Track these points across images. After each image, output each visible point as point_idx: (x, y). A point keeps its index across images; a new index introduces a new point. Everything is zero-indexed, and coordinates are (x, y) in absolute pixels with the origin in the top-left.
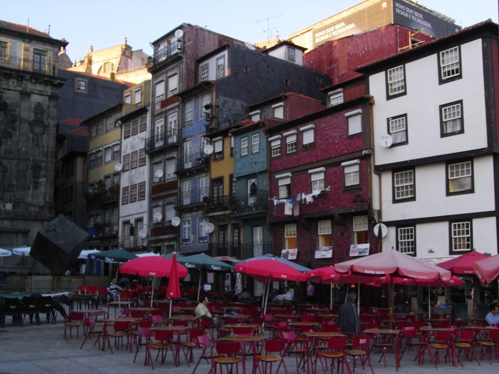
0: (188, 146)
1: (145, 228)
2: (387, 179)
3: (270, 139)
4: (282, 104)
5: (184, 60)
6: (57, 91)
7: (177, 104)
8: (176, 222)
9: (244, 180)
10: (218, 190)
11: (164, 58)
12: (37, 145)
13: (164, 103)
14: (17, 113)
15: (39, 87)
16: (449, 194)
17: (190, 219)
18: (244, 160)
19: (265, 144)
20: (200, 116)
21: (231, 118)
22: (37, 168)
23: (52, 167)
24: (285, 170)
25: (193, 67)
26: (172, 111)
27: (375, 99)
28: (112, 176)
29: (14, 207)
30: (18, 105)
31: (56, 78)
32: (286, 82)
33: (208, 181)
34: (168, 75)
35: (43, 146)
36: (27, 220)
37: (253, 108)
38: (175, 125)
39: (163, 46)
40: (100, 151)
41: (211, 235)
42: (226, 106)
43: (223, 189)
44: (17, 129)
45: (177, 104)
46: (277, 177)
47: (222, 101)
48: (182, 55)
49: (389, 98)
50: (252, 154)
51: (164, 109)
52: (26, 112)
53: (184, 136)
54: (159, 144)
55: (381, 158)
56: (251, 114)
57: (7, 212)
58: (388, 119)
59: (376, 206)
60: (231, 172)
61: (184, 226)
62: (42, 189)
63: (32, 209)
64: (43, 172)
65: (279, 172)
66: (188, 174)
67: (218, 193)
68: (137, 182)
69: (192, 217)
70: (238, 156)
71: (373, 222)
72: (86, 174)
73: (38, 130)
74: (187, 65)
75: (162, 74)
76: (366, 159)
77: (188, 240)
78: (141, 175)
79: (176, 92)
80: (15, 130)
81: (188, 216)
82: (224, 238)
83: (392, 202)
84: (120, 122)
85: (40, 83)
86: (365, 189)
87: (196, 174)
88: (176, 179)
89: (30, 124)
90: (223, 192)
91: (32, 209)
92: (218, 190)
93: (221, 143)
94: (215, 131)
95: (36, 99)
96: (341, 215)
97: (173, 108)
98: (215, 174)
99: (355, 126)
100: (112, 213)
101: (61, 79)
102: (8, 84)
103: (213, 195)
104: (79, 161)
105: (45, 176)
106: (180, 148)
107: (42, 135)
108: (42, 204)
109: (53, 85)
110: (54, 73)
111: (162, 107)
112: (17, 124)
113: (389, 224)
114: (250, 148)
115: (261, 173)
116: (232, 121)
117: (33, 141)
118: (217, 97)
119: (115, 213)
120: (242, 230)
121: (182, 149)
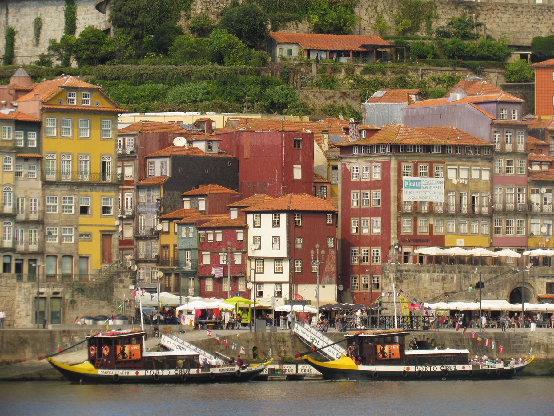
0: (142, 218)
5: (137, 158)
7: (133, 187)
8: (135, 268)
10: (166, 252)
16: (275, 273)
17: (144, 267)
19: (196, 234)
24: (206, 251)
25: (143, 162)
26: (129, 191)
33: (158, 245)
38: (131, 202)
41: (161, 279)
53: (139, 211)
55: (250, 254)
60: (175, 243)
61: (140, 271)
67: (166, 254)
69: (146, 266)
70: (180, 236)
74: (140, 161)
76: (244, 253)
77: (143, 280)
79: (132, 179)
82: (169, 281)
88: (132, 239)
90: (169, 254)
92: (166, 252)
97: (129, 189)
98: (163, 243)
99: (240, 237)
103: (162, 254)
114: (187, 233)
115: (193, 249)
118: (164, 193)
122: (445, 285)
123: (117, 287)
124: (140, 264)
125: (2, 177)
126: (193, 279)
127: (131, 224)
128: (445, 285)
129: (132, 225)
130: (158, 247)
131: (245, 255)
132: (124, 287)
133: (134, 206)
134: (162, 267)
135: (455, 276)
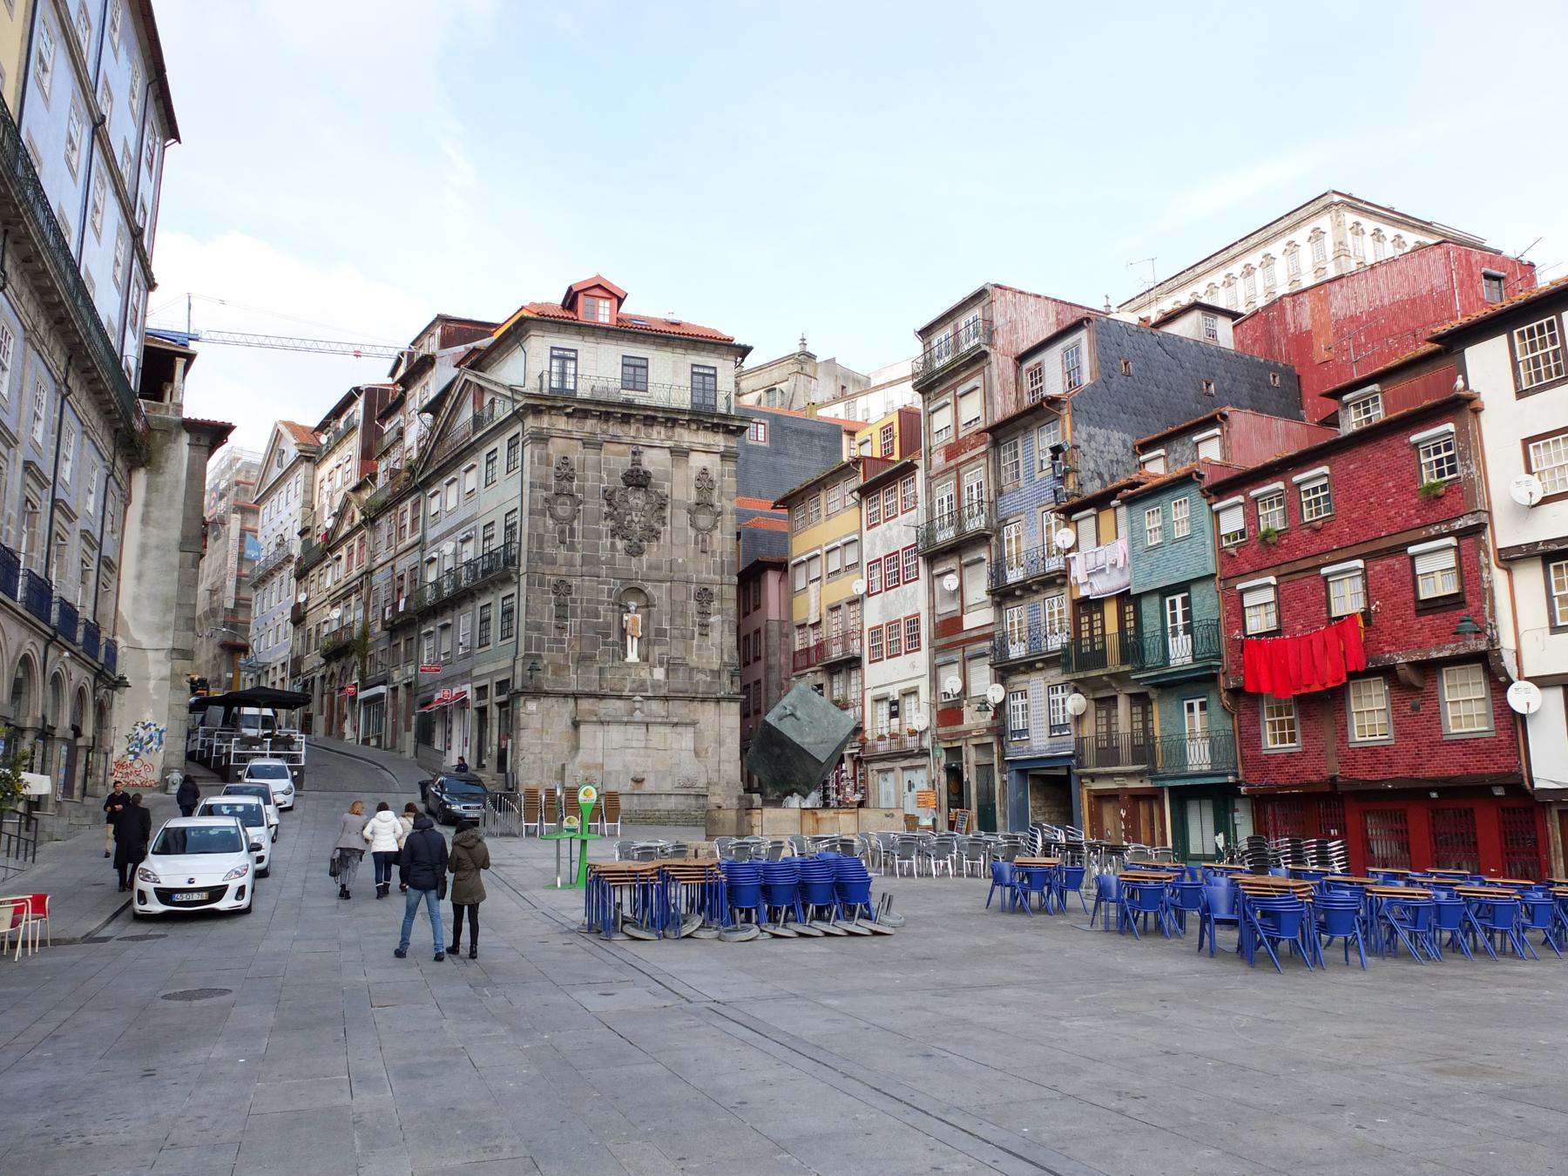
0: (1010, 532)
1: (925, 708)
2: (1530, 579)
3: (1215, 507)
4: (1217, 431)
5: (993, 358)
6: (733, 442)
9: (1156, 599)
10: (1091, 622)
11: (947, 359)
12: (704, 552)
13: (952, 451)
14: (667, 491)
15: (703, 438)
18: (1156, 555)
20: (1037, 468)
21: (1103, 470)
22: (704, 596)
23: (731, 592)
24: (1258, 571)
27: (1483, 398)
28: (844, 606)
29: (667, 676)
30: (668, 477)
31: (732, 418)
34: (959, 393)
35: (713, 552)
36: (693, 699)
37: (1145, 447)
39: (940, 336)
40: (817, 556)
41: (1078, 719)
42: (1093, 444)
43: (1103, 620)
44: (668, 520)
45: (983, 448)
46: (1239, 587)
47: (1084, 436)
48: (987, 348)
49: (1521, 394)
50: (1175, 541)
51: (952, 463)
52: (682, 490)
54: (946, 535)
55: (1506, 533)
56: (1142, 458)
57: (656, 685)
58: (1526, 442)
59: (1507, 642)
62: (715, 636)
64: (716, 604)
65: (1244, 576)
66: (1018, 593)
67: (1091, 629)
68: (901, 616)
71: (1502, 679)
72: (790, 606)
73: (704, 520)
75: (946, 391)
78: (913, 599)
79: (981, 425)
80: (664, 524)
81: (1018, 680)
82: (1109, 725)
83: (1548, 631)
84: (856, 494)
85: (706, 428)
86: (1477, 604)
87: (1037, 592)
89: (689, 511)
90: (1103, 627)
92: (1091, 622)
93: (1093, 520)
94: (1076, 500)
95: (698, 461)
96: (1416, 666)
100: (848, 680)
101: (742, 419)
102: (648, 437)
104: (772, 579)
105: (721, 611)
106: (993, 540)
107: (710, 530)
108: (716, 667)
109: (728, 431)
110: (729, 409)
111: (948, 459)
112: (668, 512)
113: (1542, 682)
114: (1165, 529)
116: (1106, 477)
117: (696, 543)
118: (1074, 429)
119: (853, 681)
120: (1155, 708)
121: (1001, 541)
124: (1014, 679)
126: (1203, 706)
127: (982, 560)
129: (985, 565)
130: (1067, 607)
131: (1481, 546)
133: (990, 503)
134: (1081, 675)
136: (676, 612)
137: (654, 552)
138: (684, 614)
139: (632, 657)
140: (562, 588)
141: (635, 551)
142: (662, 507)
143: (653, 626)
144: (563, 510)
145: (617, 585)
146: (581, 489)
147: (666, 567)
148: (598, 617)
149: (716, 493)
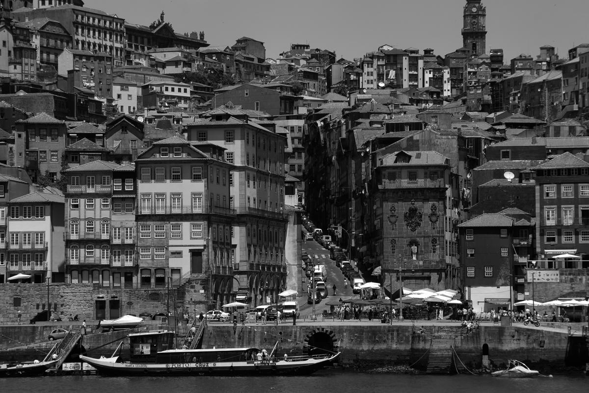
32: (518, 197)
62: (438, 252)
63: (433, 263)
64: (438, 242)
73: (434, 218)
89: (429, 217)
91: (433, 263)
105: (439, 244)
122: (573, 286)
123: (188, 291)
125: (101, 213)
128: (573, 286)
132: (195, 291)
135: (584, 278)
136: (426, 245)
137: (418, 230)
138: (428, 246)
139: (414, 258)
140: (393, 241)
141: (413, 230)
142: (421, 216)
143: (419, 250)
144: (393, 219)
145: (409, 239)
146: (397, 213)
147: (423, 233)
148: (403, 248)
149: (437, 210)
